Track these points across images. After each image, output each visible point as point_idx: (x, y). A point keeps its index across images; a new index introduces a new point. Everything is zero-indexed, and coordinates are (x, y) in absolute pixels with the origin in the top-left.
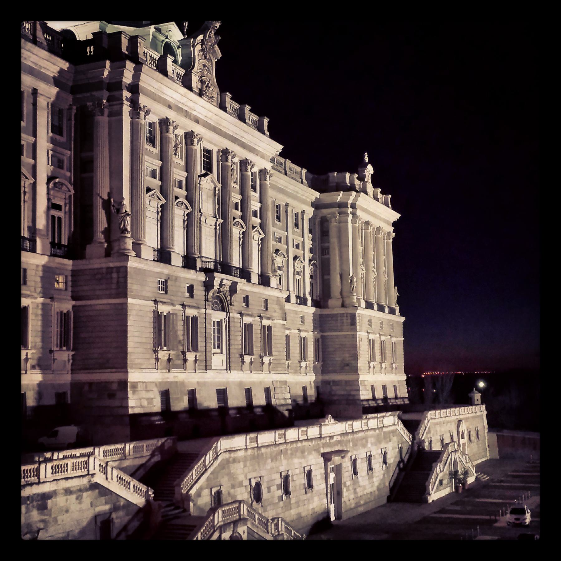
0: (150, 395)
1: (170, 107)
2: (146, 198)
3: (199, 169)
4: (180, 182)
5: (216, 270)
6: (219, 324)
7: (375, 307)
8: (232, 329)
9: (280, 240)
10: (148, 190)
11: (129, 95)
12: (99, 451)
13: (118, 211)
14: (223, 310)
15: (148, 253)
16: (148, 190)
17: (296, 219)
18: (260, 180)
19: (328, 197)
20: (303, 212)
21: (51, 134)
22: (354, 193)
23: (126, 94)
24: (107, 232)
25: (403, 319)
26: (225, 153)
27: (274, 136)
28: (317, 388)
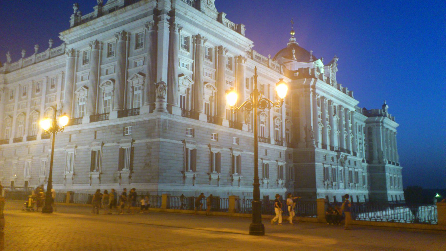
1: (324, 92)
4: (327, 118)
6: (341, 171)
7: (392, 163)
8: (346, 173)
10: (319, 123)
13: (310, 131)
14: (342, 166)
15: (320, 146)
16: (319, 123)
17: (359, 128)
18: (351, 115)
19: (371, 119)
20: (362, 125)
21: (286, 104)
22: (382, 117)
24: (306, 138)
25: (401, 168)
26: (340, 106)
28: (369, 196)
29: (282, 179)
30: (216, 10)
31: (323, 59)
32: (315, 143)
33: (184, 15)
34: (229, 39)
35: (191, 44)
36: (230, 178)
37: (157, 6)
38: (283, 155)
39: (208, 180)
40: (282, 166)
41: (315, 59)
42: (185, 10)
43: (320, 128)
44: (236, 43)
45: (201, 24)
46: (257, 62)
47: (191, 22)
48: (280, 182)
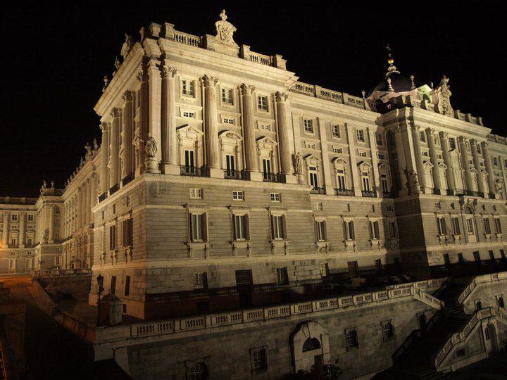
0: (439, 257)
1: (430, 123)
2: (424, 166)
3: (448, 147)
5: (464, 194)
9: (498, 175)
11: (409, 121)
12: (416, 284)
13: (411, 174)
14: (471, 213)
15: (428, 191)
16: (424, 162)
23: (408, 121)
24: (408, 184)
26: (461, 138)
27: (486, 125)
29: (378, 237)
30: (236, 44)
31: (432, 84)
32: (419, 189)
33: (180, 56)
34: (255, 74)
35: (197, 89)
36: (270, 245)
37: (145, 54)
38: (378, 208)
39: (231, 250)
40: (376, 223)
41: (418, 86)
42: (179, 50)
43: (427, 169)
44: (268, 78)
45: (207, 63)
46: (323, 99)
47: (191, 63)
48: (375, 242)
